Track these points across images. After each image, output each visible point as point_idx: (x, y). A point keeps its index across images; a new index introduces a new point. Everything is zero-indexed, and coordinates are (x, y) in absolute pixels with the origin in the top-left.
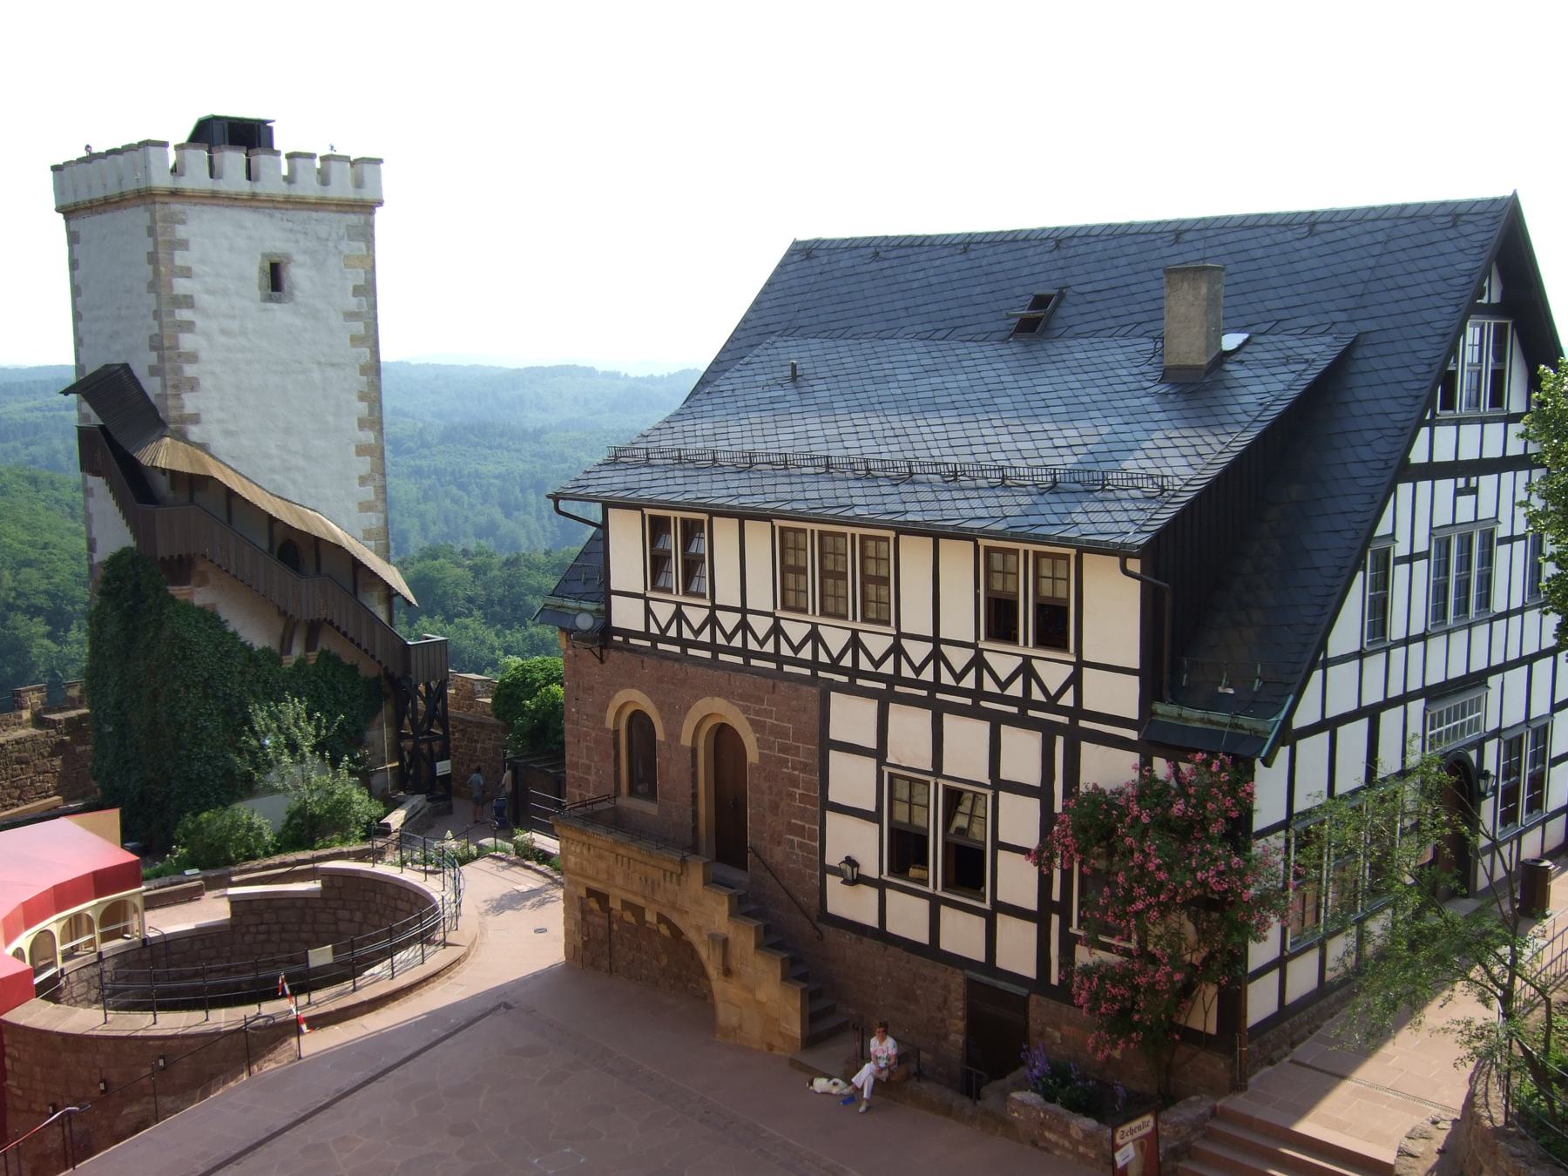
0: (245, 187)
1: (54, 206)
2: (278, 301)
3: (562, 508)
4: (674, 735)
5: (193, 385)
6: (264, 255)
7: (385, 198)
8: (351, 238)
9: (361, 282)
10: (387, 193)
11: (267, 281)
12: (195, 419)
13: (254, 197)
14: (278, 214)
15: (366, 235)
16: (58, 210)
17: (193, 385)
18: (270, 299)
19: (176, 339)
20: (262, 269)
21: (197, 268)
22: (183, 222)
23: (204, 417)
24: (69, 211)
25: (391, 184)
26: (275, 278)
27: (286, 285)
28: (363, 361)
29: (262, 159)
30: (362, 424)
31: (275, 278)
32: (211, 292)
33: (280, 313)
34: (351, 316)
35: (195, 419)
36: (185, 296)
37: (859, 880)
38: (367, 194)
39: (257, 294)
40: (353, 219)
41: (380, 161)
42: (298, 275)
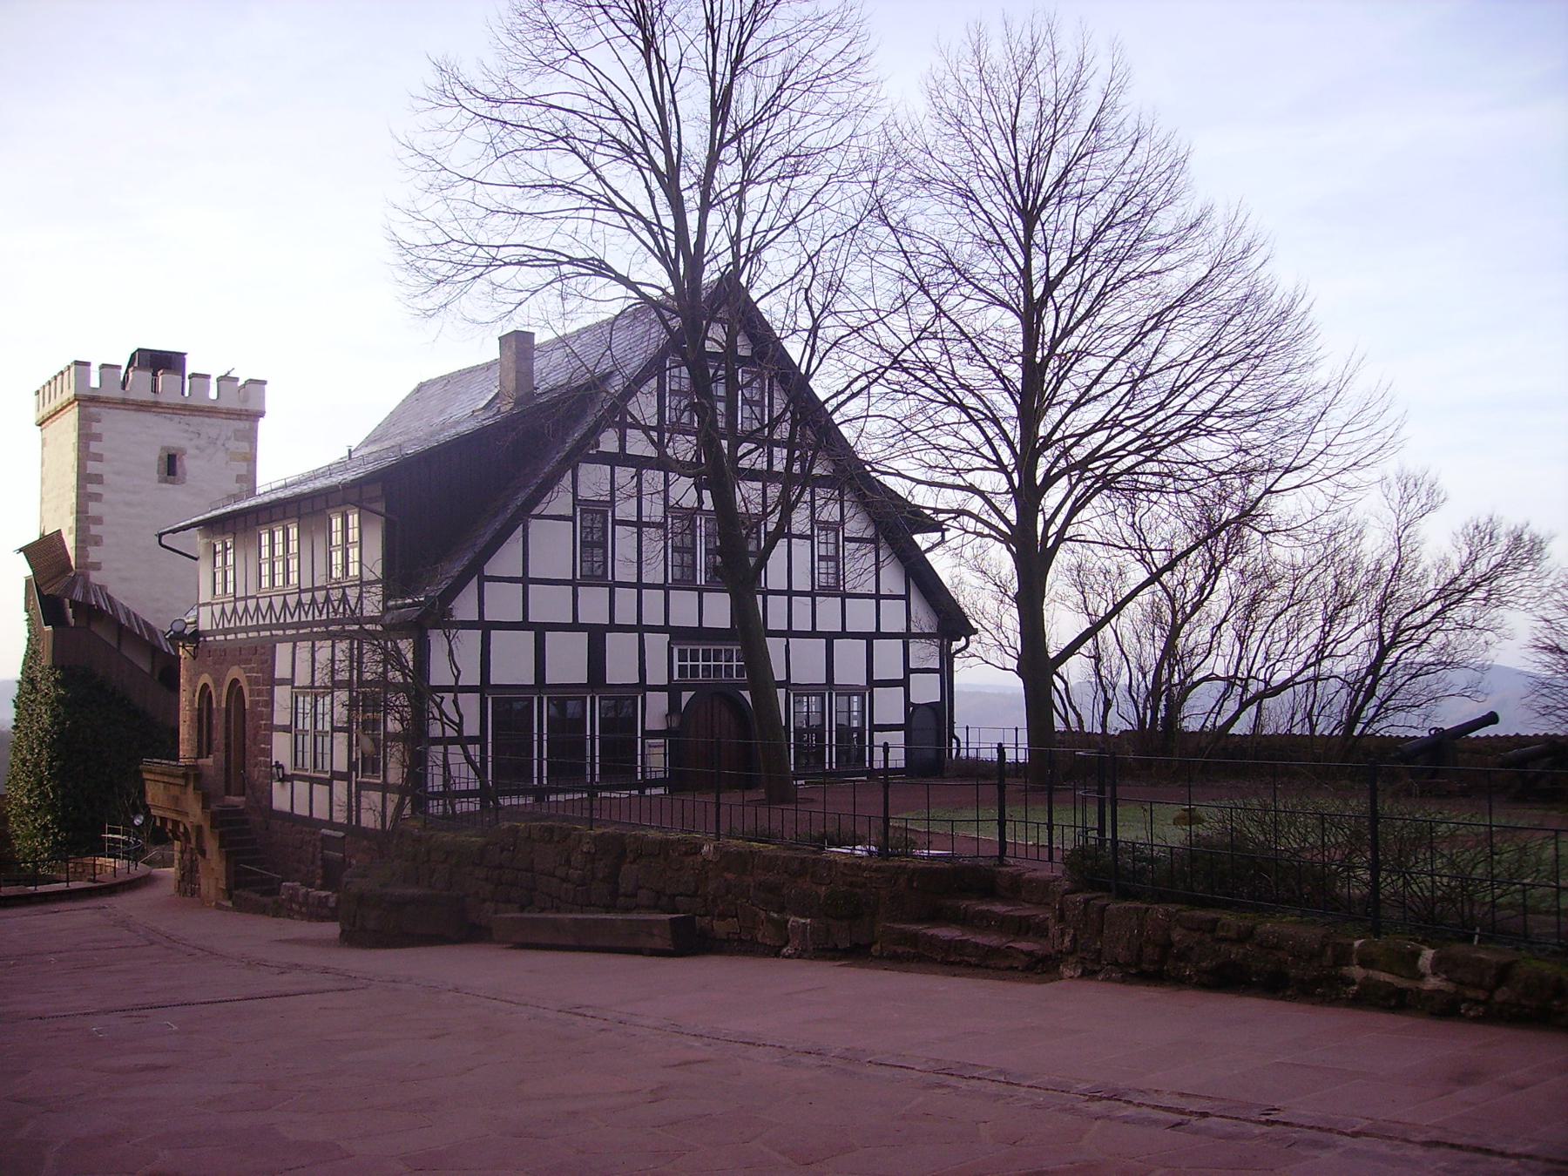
0: (148, 396)
4: (219, 703)
5: (97, 541)
7: (267, 409)
9: (243, 472)
10: (269, 406)
12: (97, 566)
13: (156, 404)
14: (177, 418)
15: (251, 438)
21: (106, 455)
25: (272, 400)
26: (171, 466)
27: (179, 471)
31: (171, 466)
32: (118, 473)
33: (173, 492)
35: (97, 566)
37: (284, 779)
38: (252, 406)
39: (156, 476)
40: (243, 425)
41: (264, 382)
42: (189, 464)
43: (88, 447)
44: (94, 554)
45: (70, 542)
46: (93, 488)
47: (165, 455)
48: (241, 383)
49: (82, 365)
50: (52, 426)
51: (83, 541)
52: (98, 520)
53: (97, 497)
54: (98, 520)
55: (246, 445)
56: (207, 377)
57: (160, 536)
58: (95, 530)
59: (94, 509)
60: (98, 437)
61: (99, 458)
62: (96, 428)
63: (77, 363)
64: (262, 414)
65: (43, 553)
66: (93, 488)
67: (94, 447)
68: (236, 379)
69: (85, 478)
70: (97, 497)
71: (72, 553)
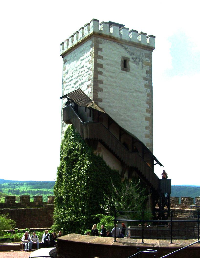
2: (126, 71)
6: (122, 57)
8: (146, 57)
11: (123, 64)
19: (97, 76)
20: (121, 61)
21: (104, 57)
22: (101, 44)
23: (103, 100)
26: (125, 64)
27: (128, 66)
28: (148, 92)
30: (147, 111)
31: (125, 64)
34: (145, 79)
41: (154, 37)
42: (131, 64)
43: (97, 53)
46: (99, 69)
51: (96, 90)
53: (101, 73)
55: (149, 59)
58: (100, 86)
59: (100, 77)
62: (100, 46)
63: (95, 20)
64: (154, 48)
66: (99, 69)
67: (100, 53)
69: (97, 65)
70: (101, 73)
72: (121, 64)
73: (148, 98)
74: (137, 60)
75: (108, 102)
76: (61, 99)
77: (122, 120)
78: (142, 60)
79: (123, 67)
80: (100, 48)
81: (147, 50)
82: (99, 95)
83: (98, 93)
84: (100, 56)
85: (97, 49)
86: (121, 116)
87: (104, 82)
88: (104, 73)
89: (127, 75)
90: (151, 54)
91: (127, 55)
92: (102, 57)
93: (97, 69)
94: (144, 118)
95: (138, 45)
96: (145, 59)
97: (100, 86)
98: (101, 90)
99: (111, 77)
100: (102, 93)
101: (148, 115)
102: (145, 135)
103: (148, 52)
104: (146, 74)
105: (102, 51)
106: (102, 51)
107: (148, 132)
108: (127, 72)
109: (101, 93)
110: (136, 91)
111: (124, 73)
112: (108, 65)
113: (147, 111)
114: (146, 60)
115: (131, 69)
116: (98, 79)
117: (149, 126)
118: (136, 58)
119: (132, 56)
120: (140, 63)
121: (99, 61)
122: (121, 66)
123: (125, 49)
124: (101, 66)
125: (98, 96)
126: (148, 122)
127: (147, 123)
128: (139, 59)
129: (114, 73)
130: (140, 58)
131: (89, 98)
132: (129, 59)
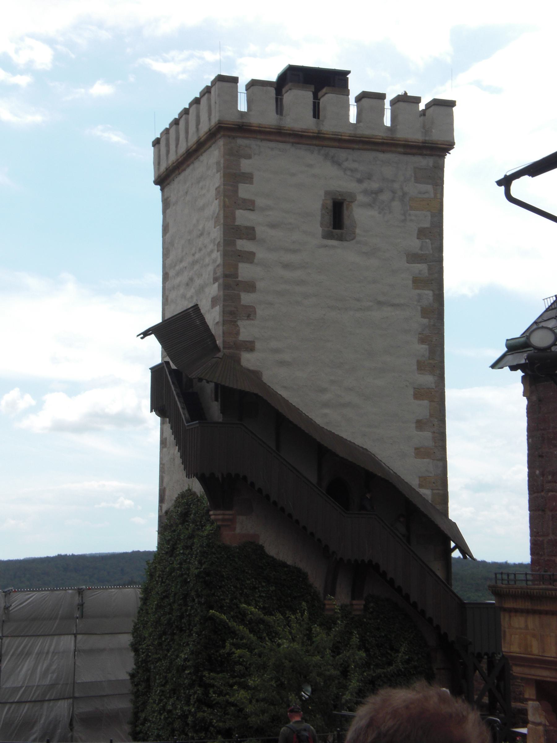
1: (152, 178)
2: (340, 238)
3: (514, 193)
6: (327, 193)
8: (417, 181)
9: (426, 224)
11: (329, 218)
12: (250, 347)
15: (436, 178)
16: (156, 182)
17: (250, 313)
18: (328, 236)
19: (236, 268)
20: (324, 206)
21: (260, 202)
22: (249, 157)
23: (258, 345)
24: (162, 180)
26: (337, 216)
27: (347, 222)
29: (328, 99)
30: (421, 367)
31: (337, 216)
34: (413, 258)
35: (250, 347)
36: (247, 228)
38: (436, 136)
39: (320, 230)
41: (451, 104)
42: (360, 215)
43: (236, 191)
44: (246, 330)
45: (213, 317)
46: (243, 245)
47: (330, 203)
48: (422, 106)
49: (226, 82)
50: (178, 184)
51: (232, 313)
52: (250, 287)
53: (249, 257)
54: (250, 287)
55: (429, 188)
56: (381, 97)
57: (505, 182)
58: (246, 298)
59: (245, 271)
60: (248, 178)
61: (249, 205)
62: (246, 165)
63: (220, 79)
64: (449, 146)
65: (178, 332)
66: (243, 245)
67: (244, 191)
68: (417, 100)
69: (234, 233)
70: (249, 257)
71: (217, 331)
72: (323, 216)
73: (426, 321)
74: (385, 197)
75: (276, 351)
76: (142, 338)
77: (326, 405)
78: (405, 194)
79: (331, 229)
80: (243, 173)
81: (421, 154)
82: (242, 330)
83: (240, 323)
84: (244, 200)
85: (234, 178)
86: (323, 390)
87: (260, 285)
88: (261, 254)
89: (344, 253)
90: (439, 169)
91: (343, 183)
92: (253, 202)
93: (234, 243)
94: (412, 392)
95: (388, 144)
96: (414, 189)
97: (246, 298)
98: (250, 313)
99: (286, 266)
100: (252, 322)
101: (428, 380)
102: (416, 449)
103: (426, 162)
104: (417, 241)
105: (251, 183)
106: (251, 183)
107: (425, 437)
108: (345, 244)
109: (248, 322)
110: (380, 303)
111: (334, 247)
112: (273, 226)
113: (421, 367)
114: (420, 193)
115: (358, 231)
116: (240, 279)
117: (431, 416)
118: (380, 191)
119: (365, 185)
120: (396, 205)
121: (243, 217)
122: (322, 224)
123: (337, 163)
124: (249, 233)
125: (238, 333)
126: (426, 403)
127: (422, 408)
128: (394, 192)
129: (294, 251)
130: (396, 186)
131: (212, 337)
132: (352, 197)
